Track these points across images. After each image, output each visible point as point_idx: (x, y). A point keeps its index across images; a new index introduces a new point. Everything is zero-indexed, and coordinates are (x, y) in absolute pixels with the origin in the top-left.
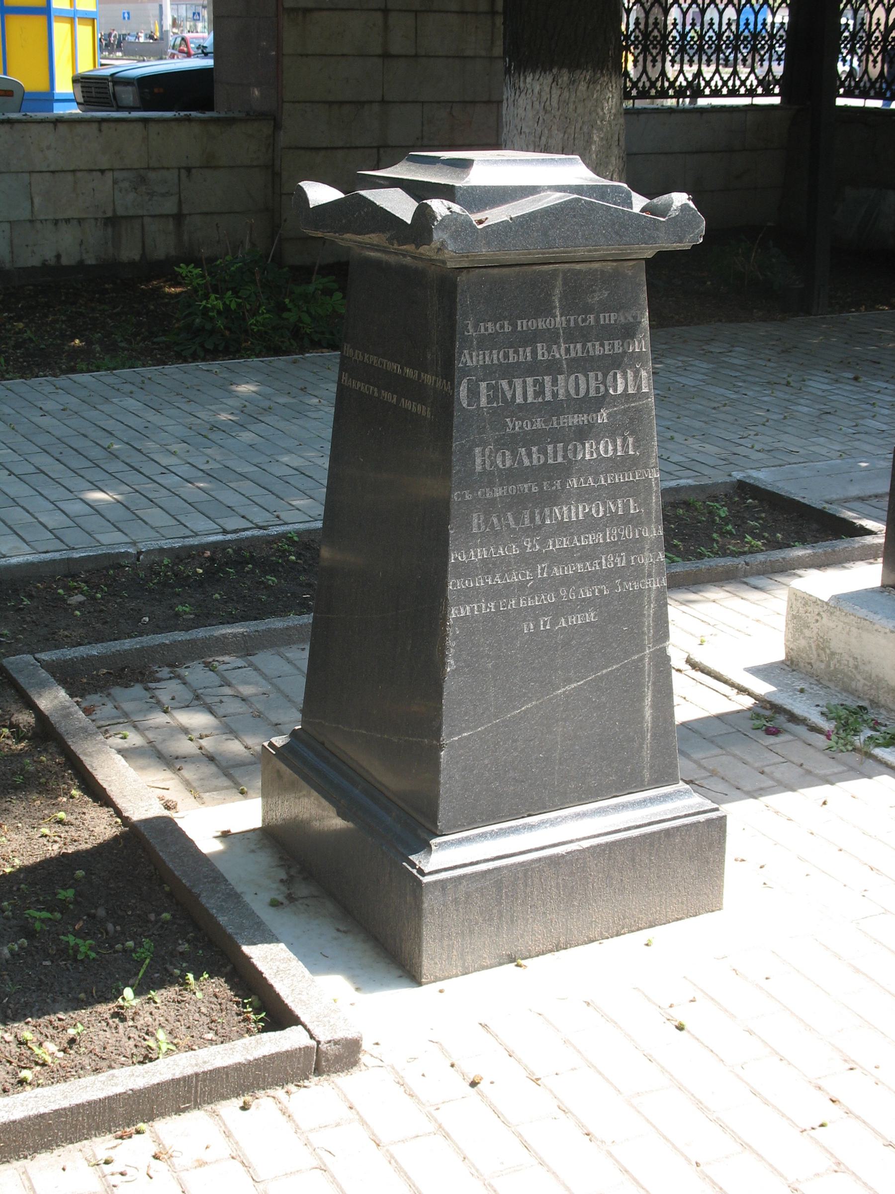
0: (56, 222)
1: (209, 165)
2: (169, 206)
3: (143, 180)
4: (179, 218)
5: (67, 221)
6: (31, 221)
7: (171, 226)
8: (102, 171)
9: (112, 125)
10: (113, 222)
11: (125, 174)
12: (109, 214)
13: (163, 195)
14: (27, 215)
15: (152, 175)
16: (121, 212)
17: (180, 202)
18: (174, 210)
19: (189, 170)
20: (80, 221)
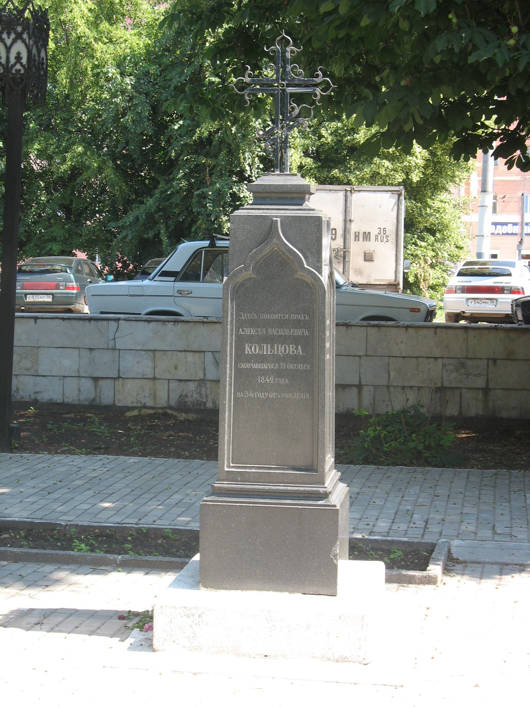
0: (403, 388)
1: (510, 357)
2: (480, 383)
3: (463, 365)
4: (486, 391)
5: (411, 387)
6: (388, 387)
7: (480, 395)
8: (436, 358)
9: (444, 330)
10: (441, 390)
11: (451, 361)
12: (439, 385)
13: (476, 376)
14: (385, 383)
15: (469, 362)
16: (446, 384)
17: (487, 382)
18: (483, 385)
19: (495, 360)
20: (419, 388)
